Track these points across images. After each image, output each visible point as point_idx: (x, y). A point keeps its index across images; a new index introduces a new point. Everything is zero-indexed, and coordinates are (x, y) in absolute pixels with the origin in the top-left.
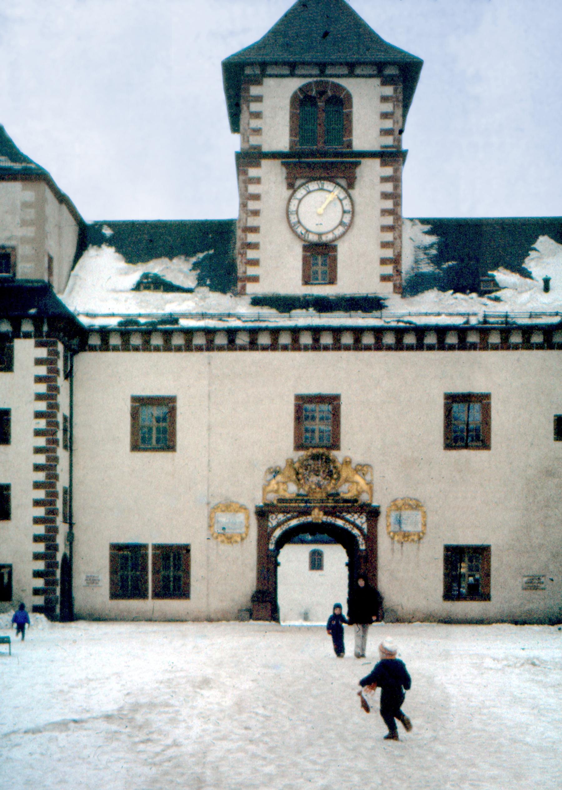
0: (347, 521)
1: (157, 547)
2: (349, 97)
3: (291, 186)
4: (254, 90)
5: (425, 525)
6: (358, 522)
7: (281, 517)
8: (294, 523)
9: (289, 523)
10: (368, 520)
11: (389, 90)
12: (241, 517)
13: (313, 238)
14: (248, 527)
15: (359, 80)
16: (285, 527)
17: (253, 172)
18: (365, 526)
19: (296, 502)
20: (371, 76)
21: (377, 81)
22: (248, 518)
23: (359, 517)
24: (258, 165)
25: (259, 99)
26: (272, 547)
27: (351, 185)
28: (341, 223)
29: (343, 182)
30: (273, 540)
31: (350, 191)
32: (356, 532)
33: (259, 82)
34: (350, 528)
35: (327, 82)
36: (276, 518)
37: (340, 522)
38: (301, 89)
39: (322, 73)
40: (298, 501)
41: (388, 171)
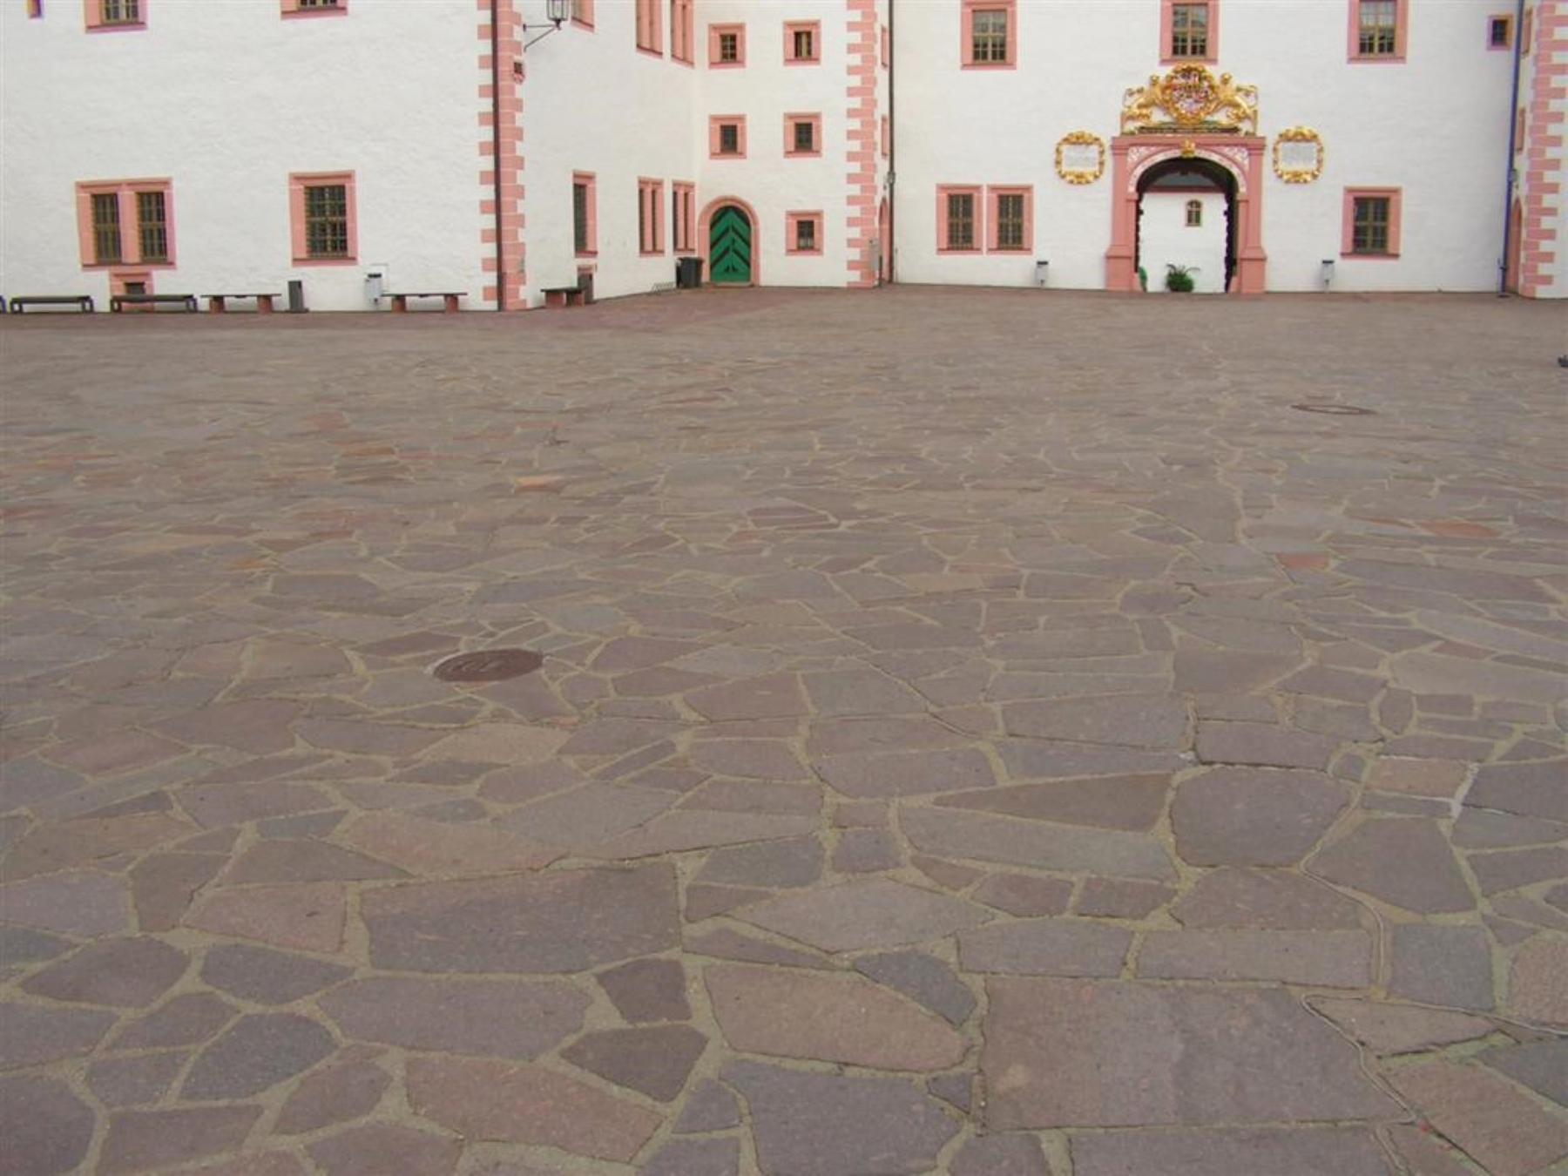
0: (1224, 156)
1: (993, 189)
5: (1320, 162)
6: (1238, 158)
7: (1143, 151)
10: (1250, 155)
14: (1102, 164)
16: (1148, 164)
18: (1246, 162)
19: (1162, 132)
22: (1102, 153)
26: (1132, 189)
30: (1134, 181)
32: (1235, 171)
36: (1138, 151)
37: (1215, 158)
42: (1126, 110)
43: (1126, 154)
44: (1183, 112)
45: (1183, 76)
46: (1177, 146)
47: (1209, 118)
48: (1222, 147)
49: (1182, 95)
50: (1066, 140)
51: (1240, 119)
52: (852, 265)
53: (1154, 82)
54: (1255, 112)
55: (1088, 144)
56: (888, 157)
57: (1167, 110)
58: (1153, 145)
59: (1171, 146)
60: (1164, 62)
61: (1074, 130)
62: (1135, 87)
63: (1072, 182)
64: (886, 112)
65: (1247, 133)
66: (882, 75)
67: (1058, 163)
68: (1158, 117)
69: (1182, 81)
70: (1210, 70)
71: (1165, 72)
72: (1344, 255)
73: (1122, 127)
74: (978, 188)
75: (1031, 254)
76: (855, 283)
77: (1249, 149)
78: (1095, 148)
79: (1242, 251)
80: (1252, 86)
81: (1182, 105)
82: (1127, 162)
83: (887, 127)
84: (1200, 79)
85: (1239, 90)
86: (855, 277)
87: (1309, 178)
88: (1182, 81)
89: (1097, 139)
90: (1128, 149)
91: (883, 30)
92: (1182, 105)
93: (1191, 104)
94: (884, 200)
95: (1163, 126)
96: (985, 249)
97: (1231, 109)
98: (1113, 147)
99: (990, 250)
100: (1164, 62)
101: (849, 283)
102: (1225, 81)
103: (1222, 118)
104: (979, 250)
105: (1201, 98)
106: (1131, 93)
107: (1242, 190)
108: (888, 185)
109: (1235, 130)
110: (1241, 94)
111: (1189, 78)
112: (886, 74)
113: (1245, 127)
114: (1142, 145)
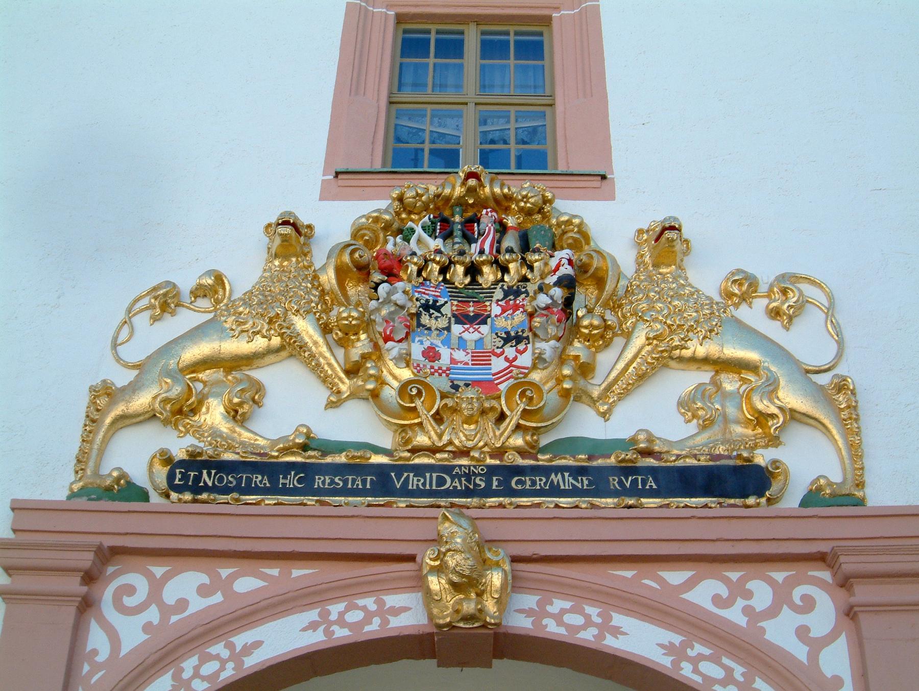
9: (241, 640)
10: (850, 613)
23: (781, 598)
42: (122, 378)
43: (86, 605)
44: (440, 383)
48: (675, 577)
49: (431, 307)
54: (841, 386)
65: (812, 498)
77: (845, 583)
81: (431, 354)
84: (525, 246)
90: (89, 578)
92: (431, 354)
93: (481, 358)
95: (312, 458)
97: (704, 376)
111: (469, 239)
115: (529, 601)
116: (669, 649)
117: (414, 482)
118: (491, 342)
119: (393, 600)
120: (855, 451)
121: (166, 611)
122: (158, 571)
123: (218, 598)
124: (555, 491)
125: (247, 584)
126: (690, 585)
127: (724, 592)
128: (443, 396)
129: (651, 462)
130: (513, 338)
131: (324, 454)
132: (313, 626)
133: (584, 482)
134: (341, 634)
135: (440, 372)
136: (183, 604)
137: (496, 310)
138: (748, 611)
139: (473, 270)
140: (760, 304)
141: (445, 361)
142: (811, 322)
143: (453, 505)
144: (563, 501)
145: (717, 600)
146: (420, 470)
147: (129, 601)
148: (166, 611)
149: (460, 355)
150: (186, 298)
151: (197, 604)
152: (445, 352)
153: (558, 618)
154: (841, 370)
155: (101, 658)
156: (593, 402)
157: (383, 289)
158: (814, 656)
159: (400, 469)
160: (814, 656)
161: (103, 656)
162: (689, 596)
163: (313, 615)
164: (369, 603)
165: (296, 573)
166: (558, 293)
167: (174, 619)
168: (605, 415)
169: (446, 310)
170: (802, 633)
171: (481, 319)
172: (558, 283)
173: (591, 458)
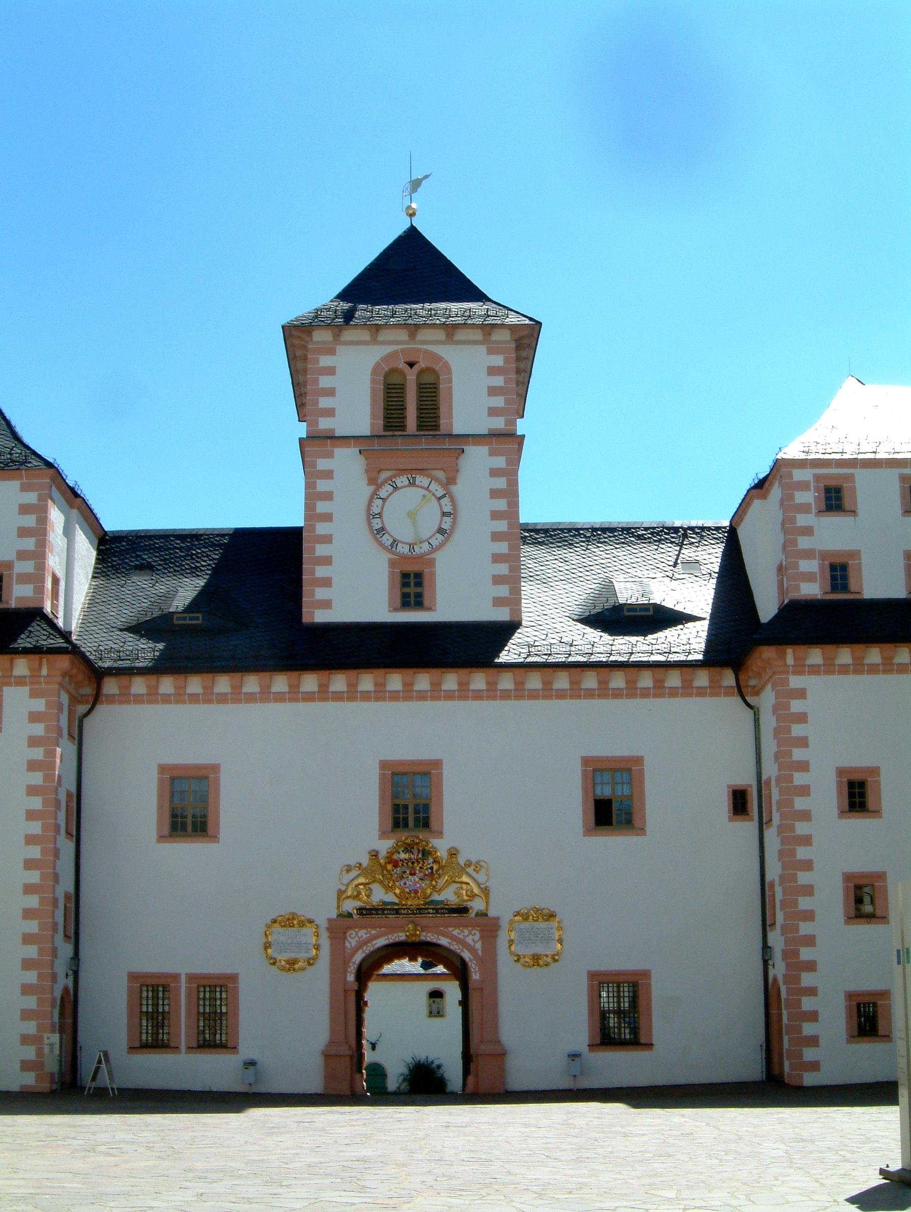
1: (191, 978)
2: (447, 368)
3: (372, 481)
4: (325, 361)
6: (469, 940)
8: (382, 942)
10: (482, 937)
11: (498, 360)
12: (307, 935)
13: (403, 549)
14: (317, 947)
15: (459, 347)
16: (368, 949)
17: (322, 464)
18: (478, 946)
20: (475, 342)
21: (483, 349)
23: (470, 933)
24: (330, 455)
25: (330, 371)
26: (351, 978)
27: (451, 480)
28: (441, 531)
29: (441, 475)
31: (453, 488)
32: (466, 955)
33: (331, 352)
34: (459, 948)
35: (419, 350)
37: (444, 941)
38: (385, 359)
39: (412, 336)
40: (385, 912)
41: (500, 462)
42: (343, 888)
43: (345, 938)
45: (406, 850)
46: (402, 929)
47: (436, 897)
48: (450, 929)
50: (275, 921)
51: (472, 896)
52: (26, 1066)
53: (374, 855)
55: (302, 924)
56: (73, 940)
57: (388, 889)
58: (373, 927)
59: (393, 929)
60: (383, 835)
61: (285, 911)
62: (352, 862)
63: (283, 969)
64: (71, 889)
65: (477, 915)
66: (67, 847)
67: (267, 946)
68: (379, 895)
69: (403, 856)
70: (435, 842)
71: (385, 846)
72: (592, 1046)
73: (338, 907)
74: (176, 977)
75: (237, 1053)
76: (31, 1086)
78: (309, 930)
79: (478, 1046)
80: (480, 861)
82: (344, 947)
83: (72, 905)
84: (423, 855)
85: (468, 864)
86: (29, 1079)
87: (549, 960)
88: (403, 856)
89: (311, 921)
90: (345, 933)
91: (69, 794)
92: (405, 884)
94: (66, 989)
96: (183, 1047)
98: (328, 929)
99: (190, 1048)
100: (383, 835)
101: (22, 1086)
102: (453, 853)
103: (449, 895)
104: (176, 1048)
105: (425, 875)
106: (349, 869)
107: (475, 975)
108: (70, 972)
109: (462, 910)
110: (470, 870)
112: (72, 845)
113: (477, 905)
114: (361, 928)
115: (424, 934)
116: (449, 943)
117: (403, 912)
118: (417, 879)
119: (400, 934)
120: (487, 903)
121: (359, 938)
122: (357, 930)
123: (368, 935)
124: (429, 913)
125: (373, 932)
126: (453, 930)
127: (459, 931)
128: (408, 893)
129: (447, 907)
130: (421, 879)
131: (386, 906)
132: (386, 940)
133: (434, 911)
134: (391, 941)
135: (407, 887)
136: (362, 936)
137: (418, 872)
138: (463, 935)
139: (413, 863)
140: (473, 867)
141: (408, 885)
142: (483, 871)
143: (410, 917)
144: (431, 915)
145: (458, 934)
146: (404, 909)
147: (352, 936)
148: (359, 938)
149: (411, 883)
150: (353, 867)
151: (365, 936)
152: (408, 882)
153: (429, 937)
154: (487, 884)
155: (349, 947)
156: (437, 892)
157: (395, 870)
158: (474, 944)
159: (400, 909)
160: (474, 944)
161: (349, 947)
162: (453, 933)
163: (386, 938)
164: (396, 935)
165: (383, 929)
166: (430, 871)
167: (361, 939)
168: (439, 895)
169: (408, 872)
170: (473, 940)
171: (414, 874)
172: (430, 868)
173: (436, 905)
